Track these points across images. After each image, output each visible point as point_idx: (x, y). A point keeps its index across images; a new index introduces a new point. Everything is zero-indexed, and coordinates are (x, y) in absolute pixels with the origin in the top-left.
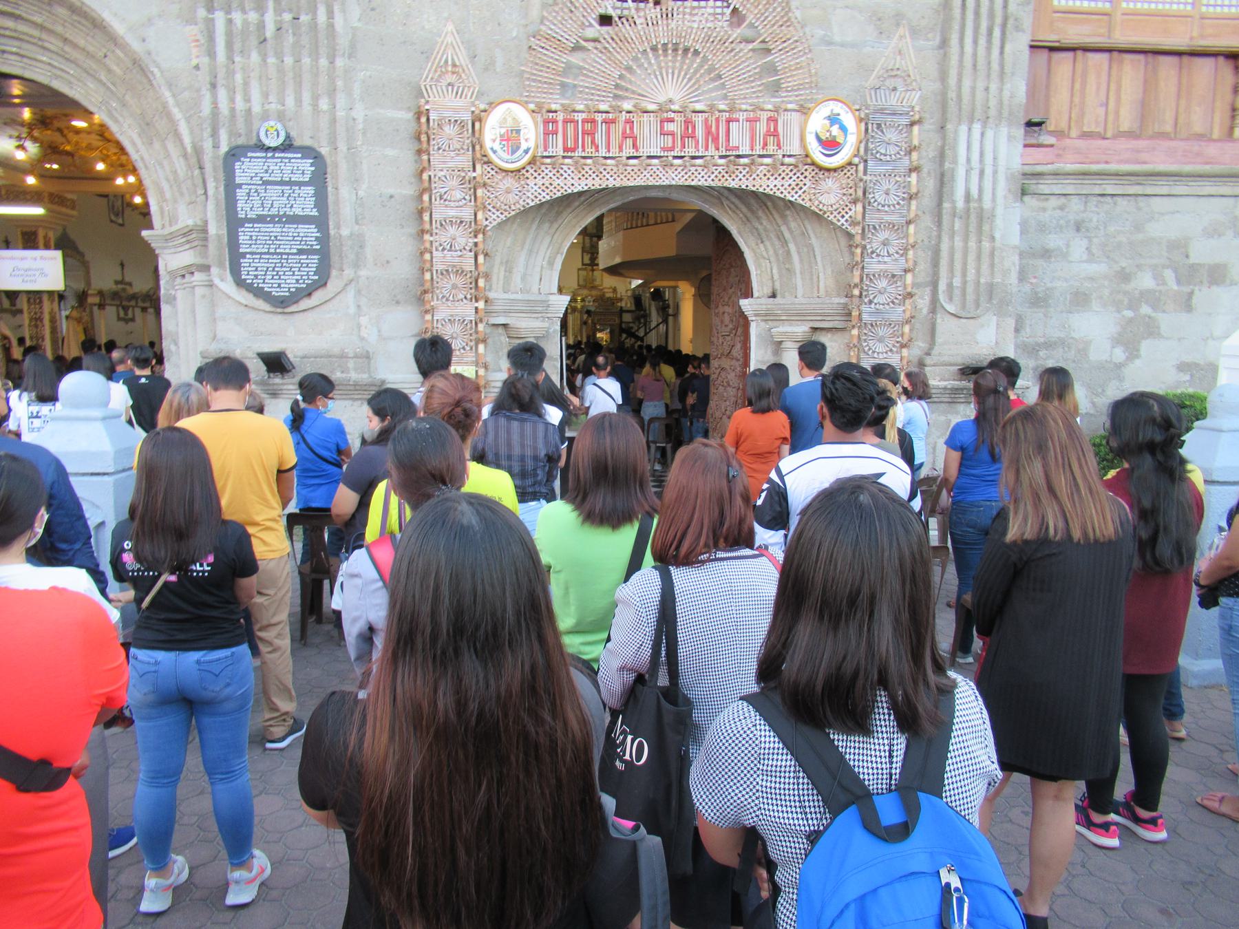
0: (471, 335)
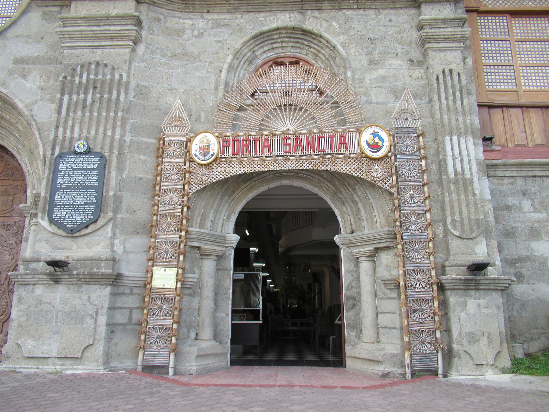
0: (176, 250)
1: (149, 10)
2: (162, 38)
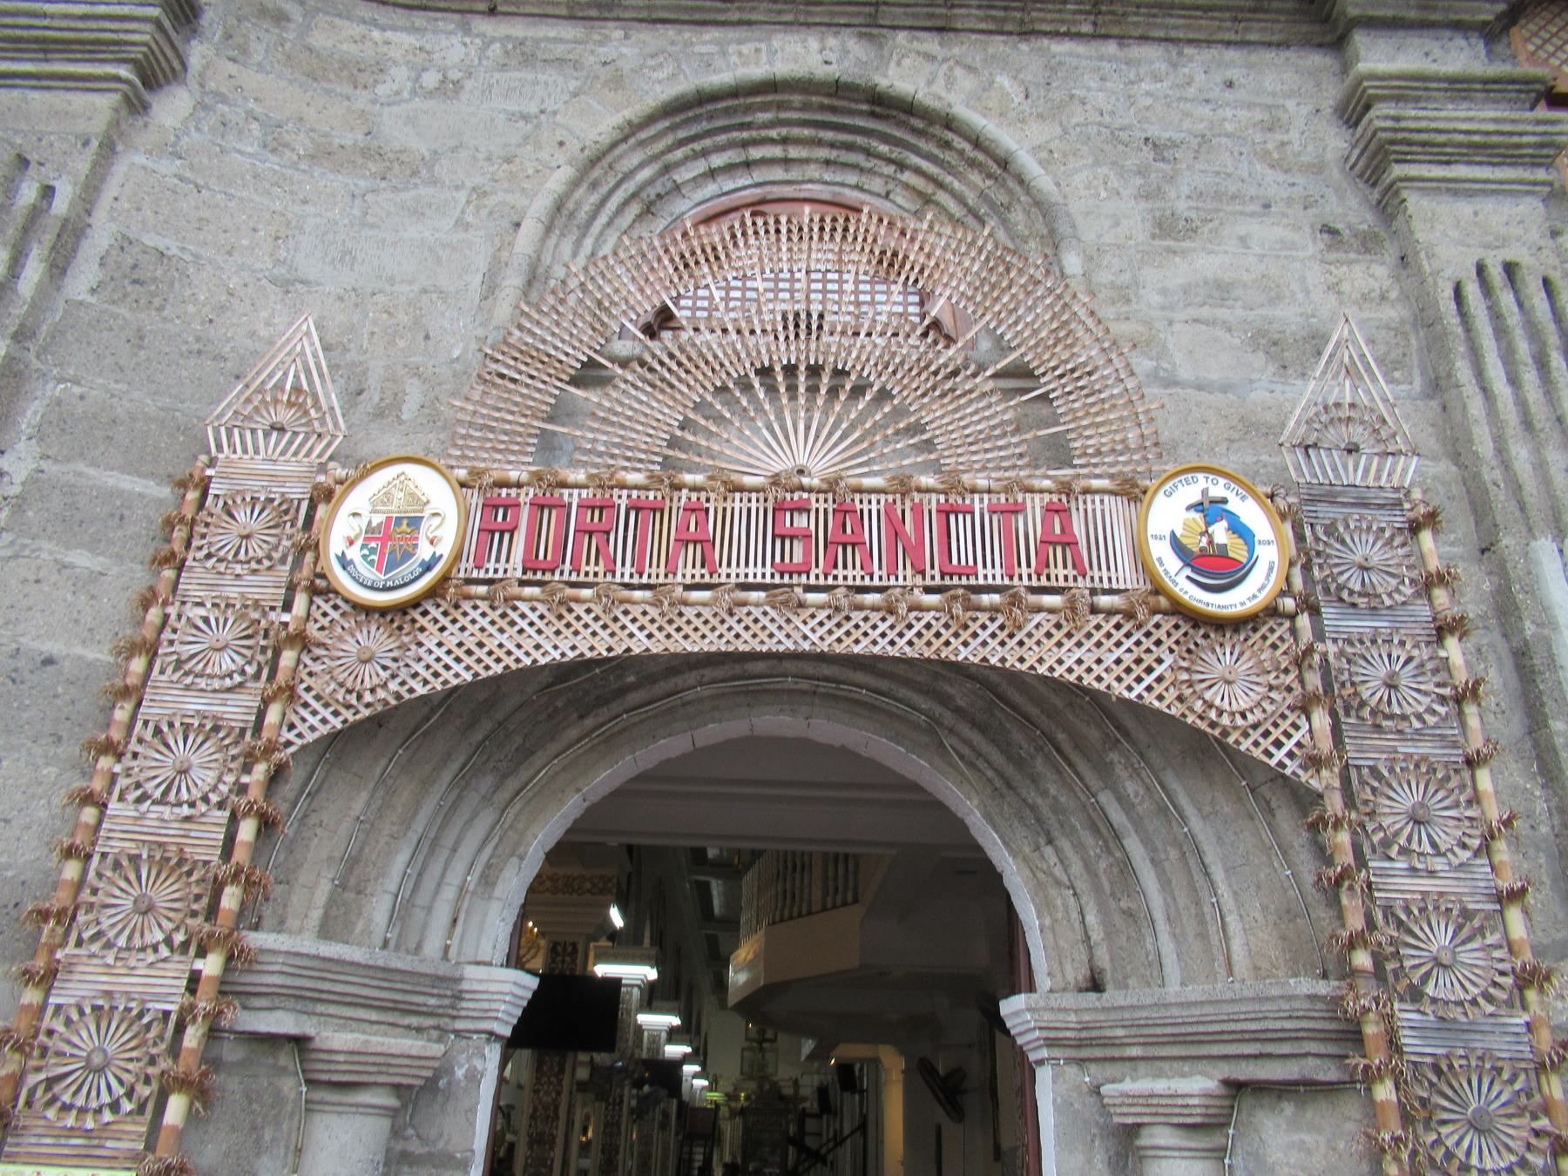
2: (284, 83)
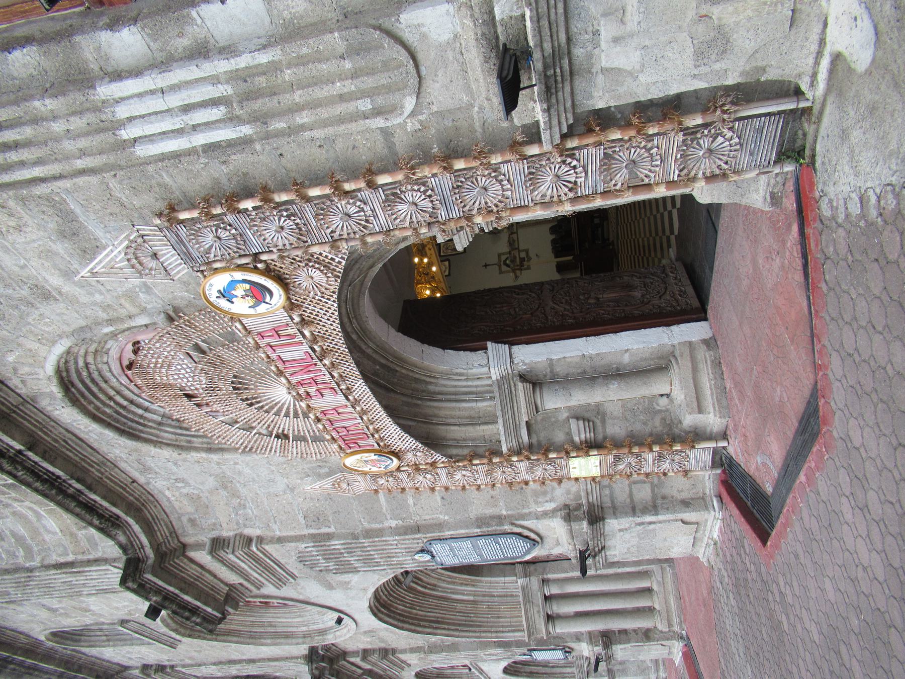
1: (185, 534)
